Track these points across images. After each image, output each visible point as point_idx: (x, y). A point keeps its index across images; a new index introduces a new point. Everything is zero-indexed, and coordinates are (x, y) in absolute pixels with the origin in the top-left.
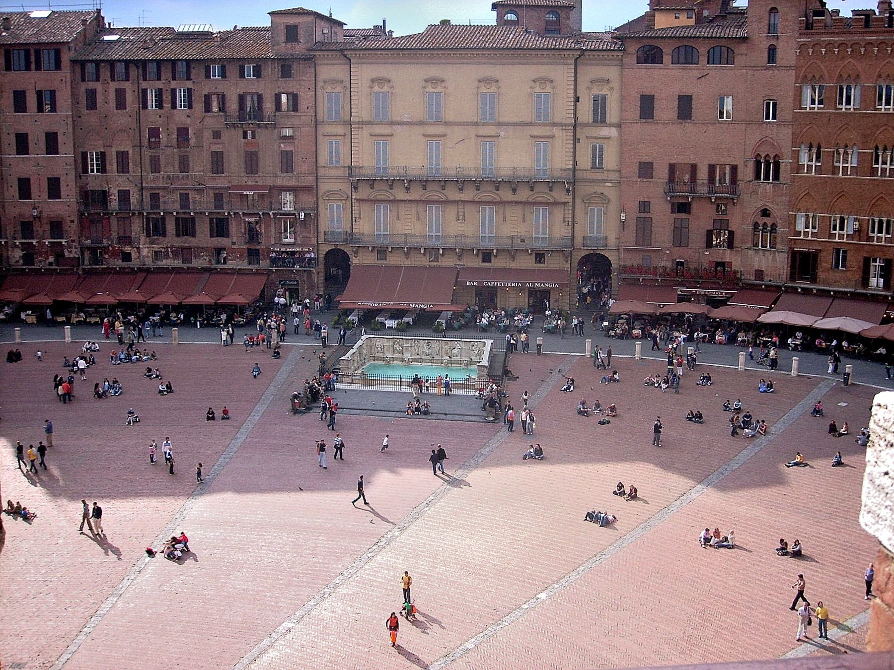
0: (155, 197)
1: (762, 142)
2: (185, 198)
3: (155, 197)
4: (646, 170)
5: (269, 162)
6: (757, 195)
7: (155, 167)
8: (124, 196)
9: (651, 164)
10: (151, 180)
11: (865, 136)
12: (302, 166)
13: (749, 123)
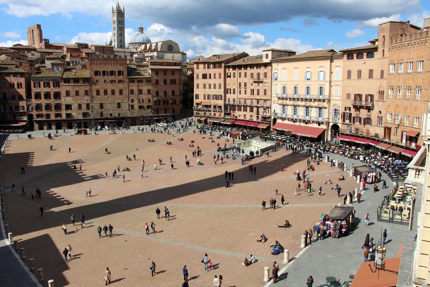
0: (240, 101)
1: (380, 86)
2: (245, 101)
3: (240, 101)
4: (348, 96)
5: (262, 92)
6: (378, 106)
7: (240, 94)
8: (234, 100)
9: (350, 94)
10: (240, 96)
11: (404, 83)
12: (268, 93)
13: (378, 79)
